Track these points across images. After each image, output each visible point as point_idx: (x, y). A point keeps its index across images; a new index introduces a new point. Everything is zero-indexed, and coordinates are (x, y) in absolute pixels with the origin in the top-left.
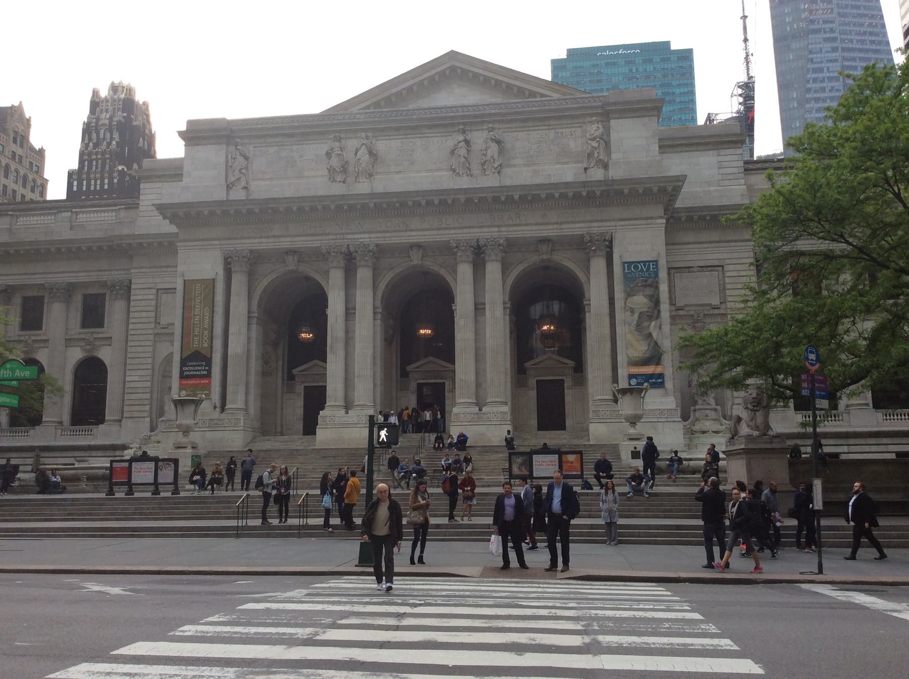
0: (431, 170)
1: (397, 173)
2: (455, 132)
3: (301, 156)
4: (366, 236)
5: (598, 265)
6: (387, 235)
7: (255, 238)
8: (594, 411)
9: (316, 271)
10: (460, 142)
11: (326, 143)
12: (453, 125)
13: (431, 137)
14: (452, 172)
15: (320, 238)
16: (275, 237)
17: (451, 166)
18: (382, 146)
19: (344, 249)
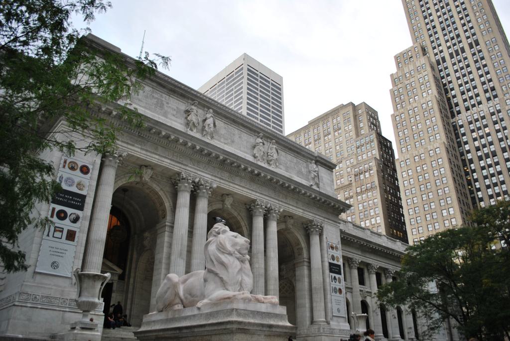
0: (242, 151)
1: (225, 143)
2: (255, 135)
3: (168, 103)
4: (210, 177)
5: (315, 240)
6: (222, 181)
7: (133, 145)
8: (323, 328)
9: (161, 189)
10: (261, 142)
11: (185, 104)
12: (255, 131)
13: (243, 132)
14: (253, 158)
15: (180, 165)
16: (147, 151)
17: (255, 154)
18: (217, 122)
19: (197, 180)
